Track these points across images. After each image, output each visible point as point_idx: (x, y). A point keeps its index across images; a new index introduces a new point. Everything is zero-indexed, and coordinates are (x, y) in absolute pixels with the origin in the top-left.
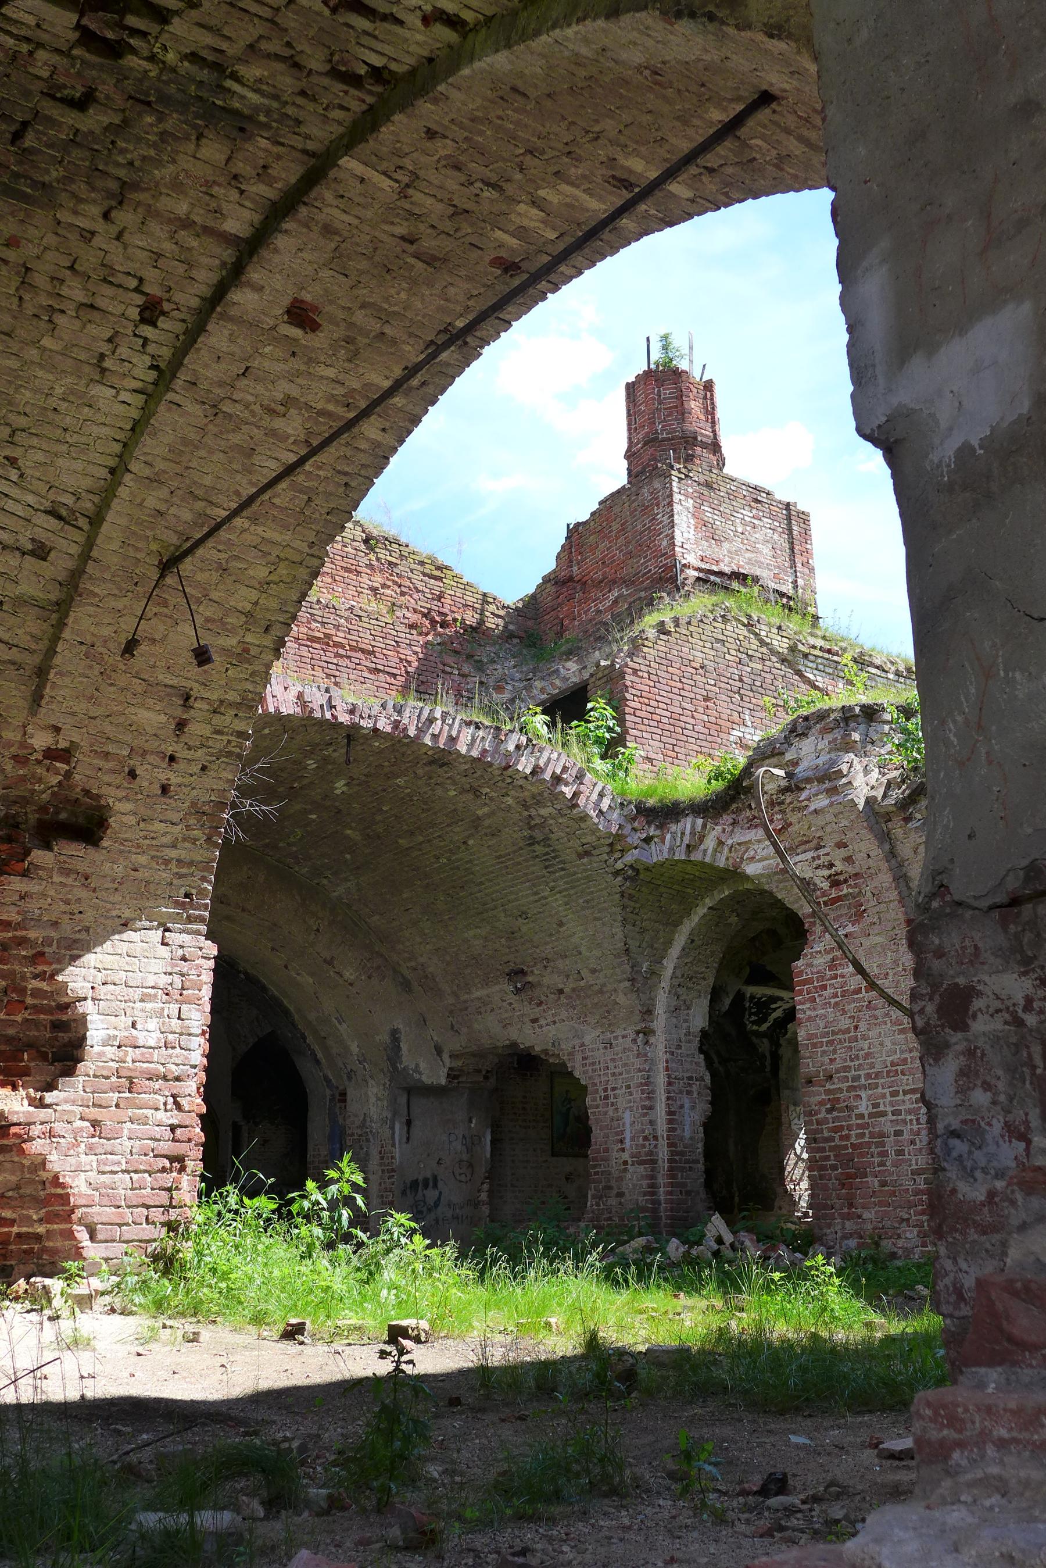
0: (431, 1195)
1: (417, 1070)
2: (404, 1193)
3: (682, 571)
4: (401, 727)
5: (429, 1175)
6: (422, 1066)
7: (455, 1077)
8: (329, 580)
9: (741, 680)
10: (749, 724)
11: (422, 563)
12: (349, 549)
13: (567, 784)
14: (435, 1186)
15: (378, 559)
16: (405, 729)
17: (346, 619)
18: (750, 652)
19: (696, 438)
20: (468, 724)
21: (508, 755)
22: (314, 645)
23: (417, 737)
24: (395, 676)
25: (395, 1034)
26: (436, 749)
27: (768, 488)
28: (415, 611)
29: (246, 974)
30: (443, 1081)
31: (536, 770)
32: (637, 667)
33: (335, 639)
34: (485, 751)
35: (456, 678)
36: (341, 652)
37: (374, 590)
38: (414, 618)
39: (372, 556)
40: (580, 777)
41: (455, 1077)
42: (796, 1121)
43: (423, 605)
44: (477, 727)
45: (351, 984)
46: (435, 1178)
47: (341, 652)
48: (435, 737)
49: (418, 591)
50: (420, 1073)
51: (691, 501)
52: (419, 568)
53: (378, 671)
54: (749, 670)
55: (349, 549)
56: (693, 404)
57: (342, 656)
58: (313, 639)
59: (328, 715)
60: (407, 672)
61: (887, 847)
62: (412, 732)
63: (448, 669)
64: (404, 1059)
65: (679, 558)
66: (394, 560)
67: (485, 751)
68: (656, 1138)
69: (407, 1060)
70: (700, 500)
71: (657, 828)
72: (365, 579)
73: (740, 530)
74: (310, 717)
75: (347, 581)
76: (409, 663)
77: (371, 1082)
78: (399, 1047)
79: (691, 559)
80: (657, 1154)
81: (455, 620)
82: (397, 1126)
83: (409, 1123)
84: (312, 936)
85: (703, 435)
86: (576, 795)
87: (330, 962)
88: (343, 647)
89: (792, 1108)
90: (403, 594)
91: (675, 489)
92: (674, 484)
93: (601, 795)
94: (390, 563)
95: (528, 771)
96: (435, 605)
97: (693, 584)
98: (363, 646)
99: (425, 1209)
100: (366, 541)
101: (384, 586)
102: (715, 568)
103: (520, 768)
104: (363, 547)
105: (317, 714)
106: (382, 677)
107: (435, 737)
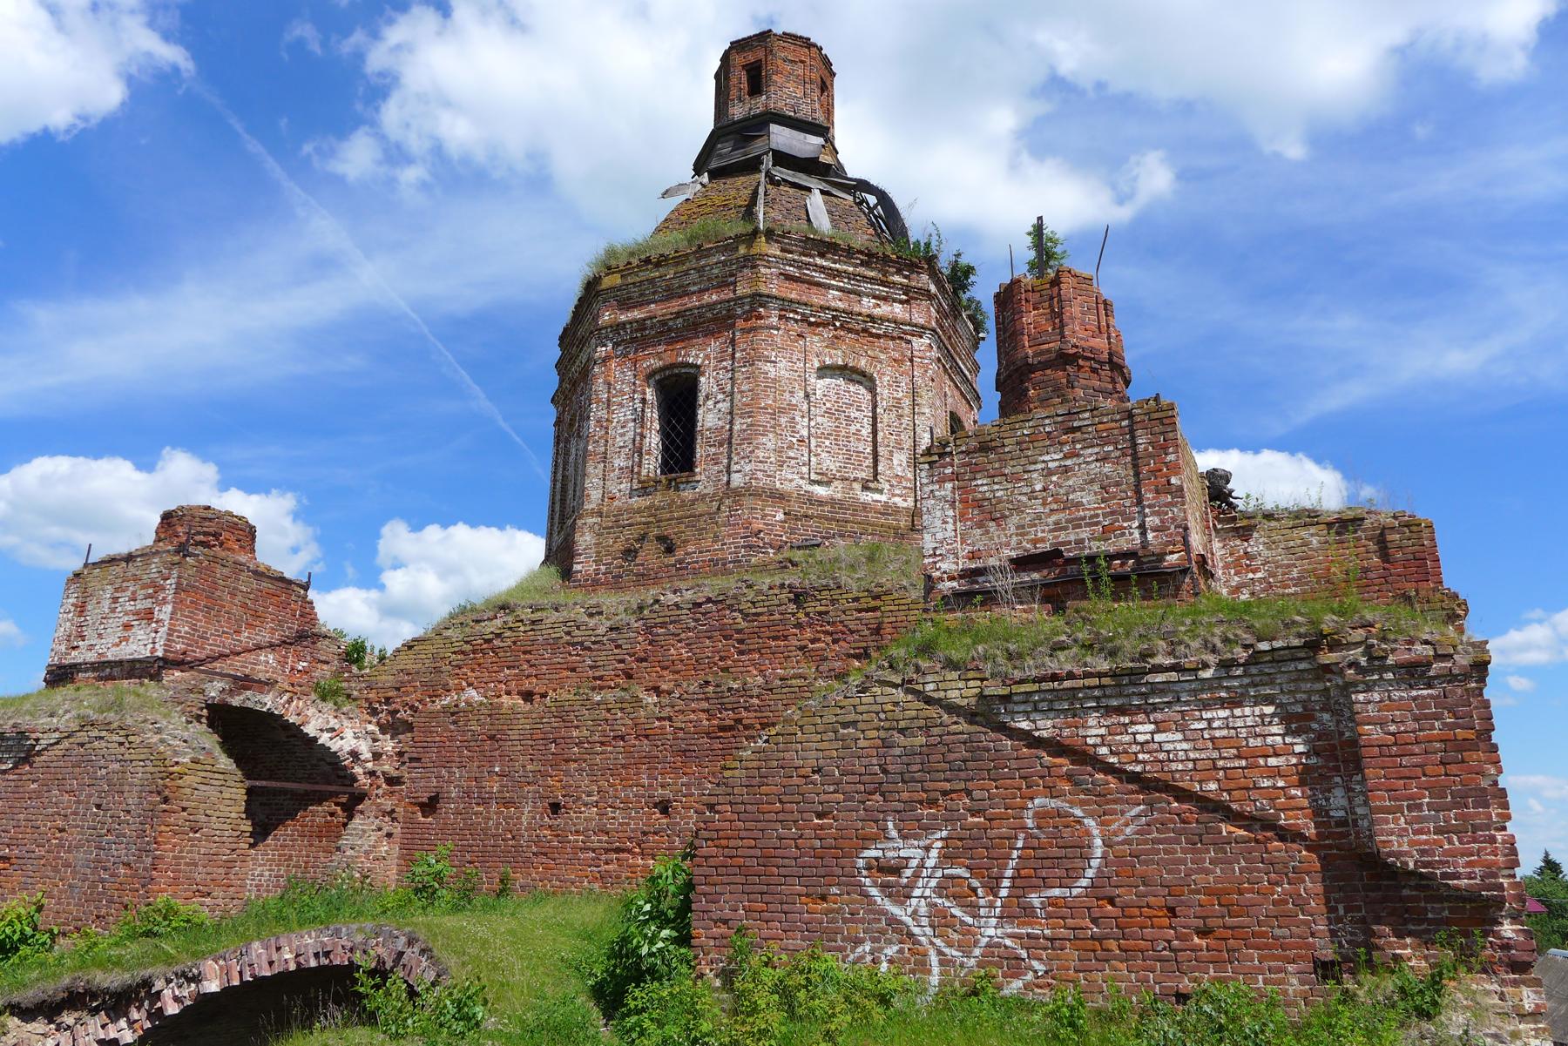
9: (885, 771)
10: (894, 834)
11: (856, 599)
12: (777, 616)
15: (807, 615)
18: (902, 724)
37: (801, 648)
49: (852, 632)
54: (897, 751)
55: (777, 616)
58: (723, 729)
73: (1038, 487)
85: (1042, 353)
90: (835, 641)
94: (820, 613)
100: (797, 595)
101: (813, 641)
104: (792, 607)
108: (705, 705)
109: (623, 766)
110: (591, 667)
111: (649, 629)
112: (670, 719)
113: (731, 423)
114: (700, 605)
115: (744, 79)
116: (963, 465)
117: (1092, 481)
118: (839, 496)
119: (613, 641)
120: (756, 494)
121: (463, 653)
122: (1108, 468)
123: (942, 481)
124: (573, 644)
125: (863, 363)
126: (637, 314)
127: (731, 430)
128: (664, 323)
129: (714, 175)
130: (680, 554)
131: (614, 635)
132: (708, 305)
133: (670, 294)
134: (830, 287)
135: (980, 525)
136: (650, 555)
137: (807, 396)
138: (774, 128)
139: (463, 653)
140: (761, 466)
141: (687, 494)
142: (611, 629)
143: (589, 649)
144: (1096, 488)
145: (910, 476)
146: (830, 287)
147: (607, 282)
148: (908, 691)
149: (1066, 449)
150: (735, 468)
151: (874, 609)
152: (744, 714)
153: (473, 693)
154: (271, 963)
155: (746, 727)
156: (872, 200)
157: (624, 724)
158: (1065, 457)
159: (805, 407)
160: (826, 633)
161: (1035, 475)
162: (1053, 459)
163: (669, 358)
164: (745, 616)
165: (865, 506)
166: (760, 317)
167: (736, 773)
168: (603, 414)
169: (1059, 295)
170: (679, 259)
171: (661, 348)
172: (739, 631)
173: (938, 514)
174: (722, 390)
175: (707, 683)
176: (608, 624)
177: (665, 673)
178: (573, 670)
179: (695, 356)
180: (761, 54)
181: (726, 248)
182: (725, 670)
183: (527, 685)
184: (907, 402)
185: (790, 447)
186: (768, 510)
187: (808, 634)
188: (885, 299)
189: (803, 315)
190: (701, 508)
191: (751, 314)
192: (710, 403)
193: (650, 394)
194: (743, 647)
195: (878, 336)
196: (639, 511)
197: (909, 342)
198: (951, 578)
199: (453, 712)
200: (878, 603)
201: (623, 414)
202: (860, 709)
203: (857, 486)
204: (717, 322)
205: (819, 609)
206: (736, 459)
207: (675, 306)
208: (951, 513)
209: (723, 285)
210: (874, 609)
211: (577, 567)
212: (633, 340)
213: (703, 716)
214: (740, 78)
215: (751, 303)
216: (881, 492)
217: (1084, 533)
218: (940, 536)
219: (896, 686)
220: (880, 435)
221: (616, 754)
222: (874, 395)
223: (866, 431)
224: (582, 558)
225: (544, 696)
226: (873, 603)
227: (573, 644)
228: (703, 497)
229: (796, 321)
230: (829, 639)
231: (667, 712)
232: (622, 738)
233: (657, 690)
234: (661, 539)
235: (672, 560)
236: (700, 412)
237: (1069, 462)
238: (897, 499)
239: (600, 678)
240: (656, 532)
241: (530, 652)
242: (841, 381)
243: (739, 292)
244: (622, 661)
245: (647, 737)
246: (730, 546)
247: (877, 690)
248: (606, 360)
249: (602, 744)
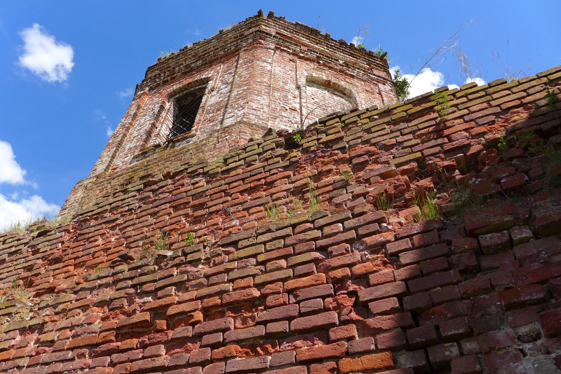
24: (322, 332)
35: (533, 247)
53: (281, 337)
55: (258, 164)
60: (362, 307)
63: (488, 239)
76: (363, 279)
81: (492, 144)
94: (328, 144)
106: (286, 352)
160: (342, 161)
229: (289, 53)
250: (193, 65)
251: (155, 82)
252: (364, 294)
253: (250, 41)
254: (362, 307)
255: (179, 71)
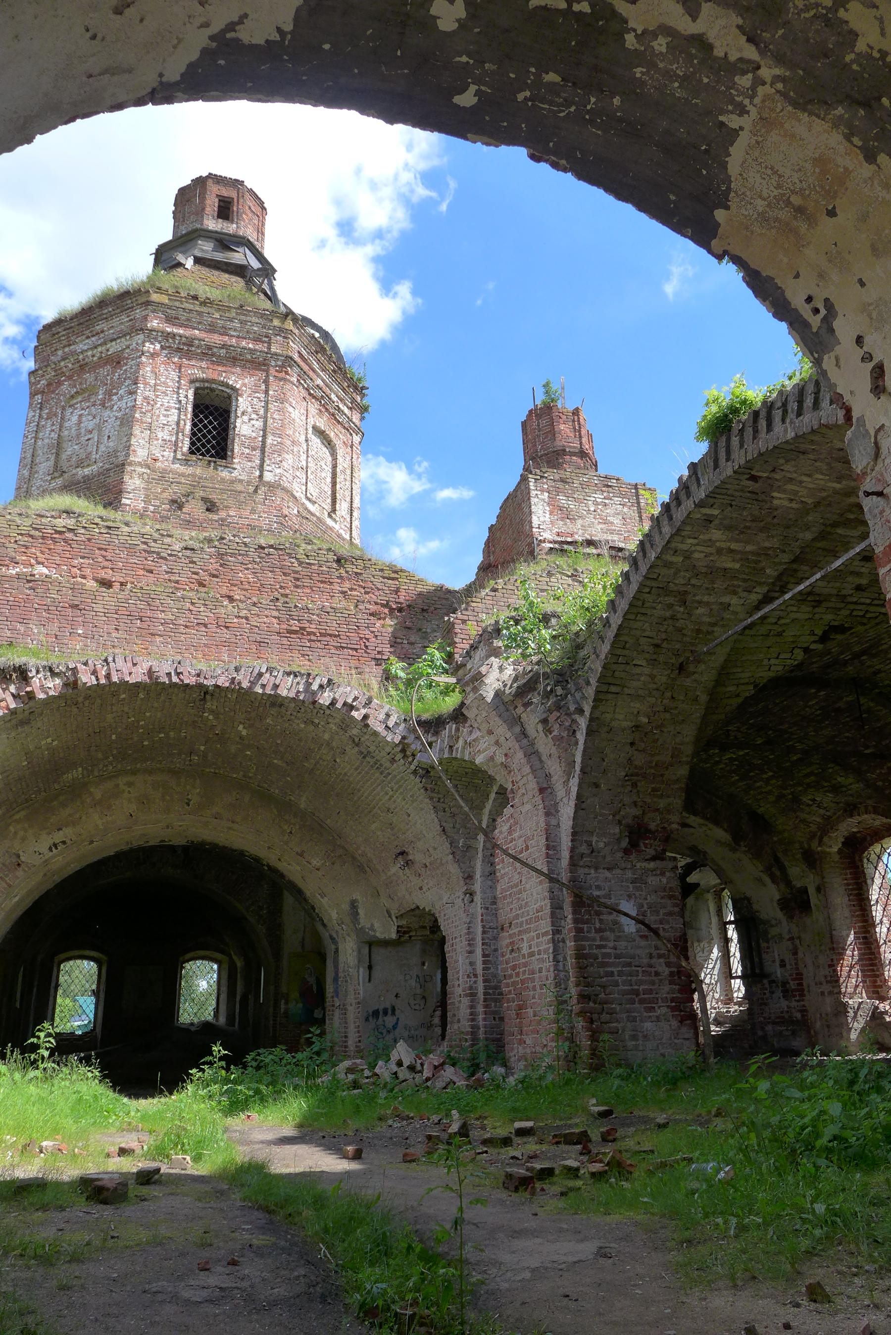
0: (390, 1020)
1: (372, 928)
2: (367, 1019)
3: (539, 545)
4: (236, 681)
5: (388, 1005)
6: (377, 925)
7: (405, 933)
8: (309, 591)
12: (324, 568)
13: (357, 710)
14: (393, 1013)
15: (347, 572)
16: (239, 683)
17: (318, 615)
19: (564, 450)
20: (289, 674)
21: (314, 693)
22: (292, 636)
23: (250, 688)
24: (356, 650)
25: (353, 905)
26: (264, 694)
27: (617, 475)
28: (376, 603)
29: (268, 866)
30: (394, 936)
31: (333, 703)
32: (466, 618)
33: (308, 630)
34: (298, 692)
35: (406, 646)
36: (313, 638)
38: (373, 608)
39: (342, 571)
40: (369, 701)
41: (405, 933)
42: (700, 954)
43: (383, 599)
44: (296, 676)
45: (318, 869)
46: (393, 1009)
47: (313, 638)
48: (263, 686)
49: (379, 590)
50: (374, 931)
51: (546, 494)
52: (380, 573)
53: (343, 648)
55: (324, 568)
56: (562, 427)
57: (314, 641)
59: (175, 679)
61: (517, 729)
62: (245, 684)
63: (398, 640)
64: (361, 921)
65: (536, 535)
66: (359, 571)
67: (298, 692)
68: (476, 976)
69: (364, 921)
70: (553, 494)
71: (433, 735)
72: (337, 587)
73: (592, 509)
74: (157, 684)
75: (322, 589)
76: (368, 639)
77: (348, 939)
78: (357, 914)
79: (547, 535)
80: (476, 988)
82: (361, 970)
83: (370, 967)
84: (286, 837)
85: (571, 447)
86: (366, 717)
87: (301, 855)
88: (315, 634)
89: (696, 944)
90: (366, 593)
91: (532, 488)
92: (531, 484)
93: (388, 715)
94: (356, 573)
95: (327, 704)
96: (392, 597)
97: (546, 554)
98: (331, 632)
99: (385, 1031)
100: (338, 561)
101: (351, 589)
102: (569, 540)
103: (321, 701)
104: (335, 565)
105: (161, 680)
107: (263, 686)
108: (276, 614)
109: (205, 645)
110: (167, 572)
111: (220, 556)
112: (247, 618)
113: (264, 436)
114: (263, 548)
115: (216, 205)
116: (552, 486)
117: (618, 514)
118: (318, 514)
119: (188, 557)
120: (284, 489)
121: (32, 536)
122: (626, 510)
123: (542, 491)
124: (149, 552)
125: (332, 435)
126: (181, 331)
127: (264, 442)
128: (210, 348)
129: (198, 261)
130: (223, 514)
131: (188, 553)
132: (249, 349)
133: (212, 329)
134: (318, 376)
135: (562, 519)
136: (195, 509)
137: (307, 441)
138: (247, 251)
139: (32, 536)
140: (285, 473)
141: (224, 474)
142: (186, 549)
143: (165, 559)
144: (621, 518)
145: (349, 520)
146: (318, 376)
147: (155, 297)
148: (573, 580)
149: (605, 494)
150: (266, 468)
151: (393, 579)
152: (307, 625)
153: (45, 571)
154: (130, 674)
155: (309, 634)
156: (317, 335)
157: (206, 615)
158: (605, 498)
159: (305, 447)
161: (590, 503)
162: (599, 497)
163: (210, 374)
164: (300, 563)
165: (331, 529)
166: (287, 373)
167: (480, 605)
168: (151, 395)
169: (579, 421)
170: (221, 307)
171: (204, 364)
172: (296, 572)
173: (541, 507)
174: (256, 412)
175: (277, 599)
176: (183, 544)
177: (235, 588)
178: (151, 572)
179: (236, 379)
180: (233, 194)
181: (262, 316)
182: (286, 596)
183: (102, 574)
184: (348, 472)
185: (298, 469)
186: (290, 504)
187: (347, 585)
188: (341, 400)
189: (308, 385)
190: (239, 487)
191: (282, 368)
192: (246, 418)
193: (191, 394)
194: (298, 583)
195: (339, 422)
196: (183, 475)
197: (351, 434)
198: (551, 542)
199: (30, 579)
200: (396, 576)
201: (170, 401)
202: (550, 584)
203: (326, 514)
204: (257, 364)
205: (355, 570)
206: (268, 462)
207: (216, 339)
208: (548, 508)
209: (257, 340)
210: (393, 579)
211: (124, 501)
212: (179, 350)
213: (275, 621)
214: (212, 204)
215: (284, 361)
216: (336, 521)
217: (616, 538)
218: (542, 519)
219: (568, 576)
220: (338, 486)
221: (198, 636)
222: (335, 459)
223: (329, 480)
224: (131, 496)
225: (122, 584)
226: (393, 575)
227: (149, 552)
228: (241, 481)
230: (363, 591)
231: (243, 613)
232: (205, 626)
233: (231, 599)
234: (203, 499)
235: (216, 517)
236: (239, 421)
237: (607, 501)
238: (341, 532)
239: (177, 582)
240: (202, 494)
241: (106, 550)
242: (318, 441)
243: (273, 349)
244: (196, 573)
245: (227, 627)
246: (265, 520)
247: (558, 576)
248: (153, 355)
249: (186, 626)
250: (215, 350)
251: (168, 340)
252: (367, 644)
253: (280, 363)
254: (366, 647)
255: (198, 347)
